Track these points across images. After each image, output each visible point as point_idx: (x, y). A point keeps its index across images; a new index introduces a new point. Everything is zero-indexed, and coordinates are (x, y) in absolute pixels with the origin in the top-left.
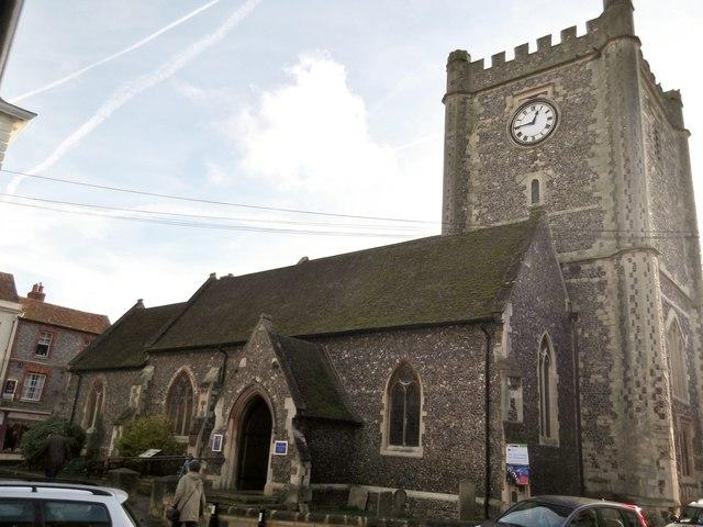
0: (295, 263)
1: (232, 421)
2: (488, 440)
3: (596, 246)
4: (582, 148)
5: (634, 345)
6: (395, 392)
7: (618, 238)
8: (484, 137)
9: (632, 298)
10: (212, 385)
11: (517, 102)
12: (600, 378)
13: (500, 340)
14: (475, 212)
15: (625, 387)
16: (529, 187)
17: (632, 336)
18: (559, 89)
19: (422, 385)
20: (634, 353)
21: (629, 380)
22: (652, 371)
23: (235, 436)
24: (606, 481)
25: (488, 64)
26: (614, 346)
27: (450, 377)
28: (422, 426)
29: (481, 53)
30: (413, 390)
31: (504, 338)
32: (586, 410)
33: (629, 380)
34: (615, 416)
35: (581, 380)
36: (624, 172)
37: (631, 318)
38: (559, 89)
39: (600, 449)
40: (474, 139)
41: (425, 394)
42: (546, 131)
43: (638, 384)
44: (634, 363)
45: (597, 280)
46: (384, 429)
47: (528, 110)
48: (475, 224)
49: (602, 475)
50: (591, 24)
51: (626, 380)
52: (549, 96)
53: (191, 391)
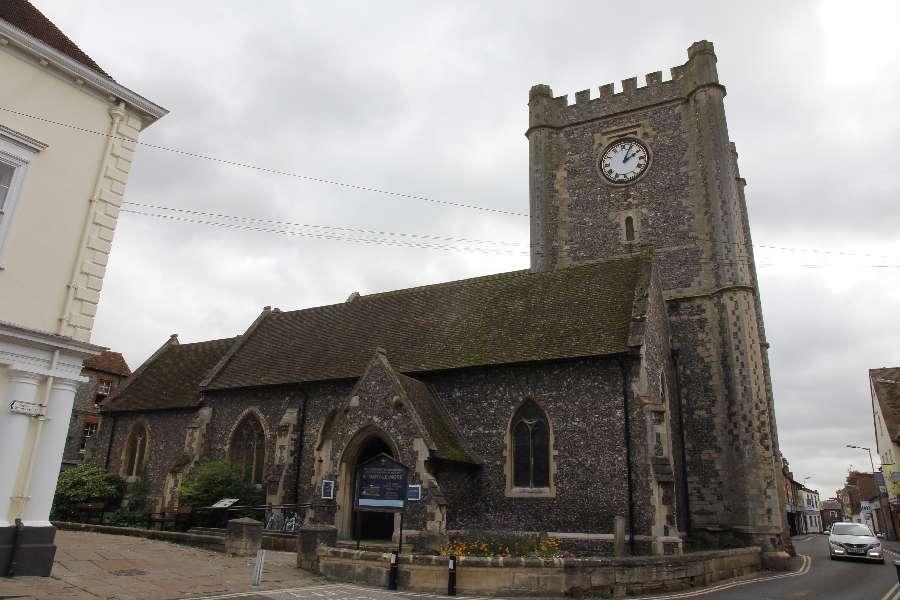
0: (343, 301)
1: (344, 465)
2: (629, 477)
4: (677, 188)
5: (738, 381)
6: (518, 430)
7: (718, 277)
8: (572, 173)
9: (735, 334)
10: (291, 429)
11: (606, 141)
12: (703, 413)
13: (637, 374)
15: (730, 422)
17: (737, 372)
18: (649, 130)
20: (739, 389)
21: (734, 414)
22: (757, 405)
23: (348, 481)
24: (712, 513)
25: (572, 101)
26: (716, 381)
27: (583, 413)
29: (565, 88)
30: (541, 430)
31: (643, 373)
32: (690, 445)
33: (734, 414)
34: (719, 450)
35: (685, 415)
36: (721, 213)
37: (735, 354)
38: (649, 130)
39: (705, 483)
40: (561, 174)
41: (555, 432)
42: (638, 170)
43: (744, 418)
44: (739, 398)
45: (697, 317)
46: (508, 470)
47: (619, 148)
48: (565, 262)
49: (709, 508)
50: (675, 71)
51: (731, 415)
53: (261, 435)
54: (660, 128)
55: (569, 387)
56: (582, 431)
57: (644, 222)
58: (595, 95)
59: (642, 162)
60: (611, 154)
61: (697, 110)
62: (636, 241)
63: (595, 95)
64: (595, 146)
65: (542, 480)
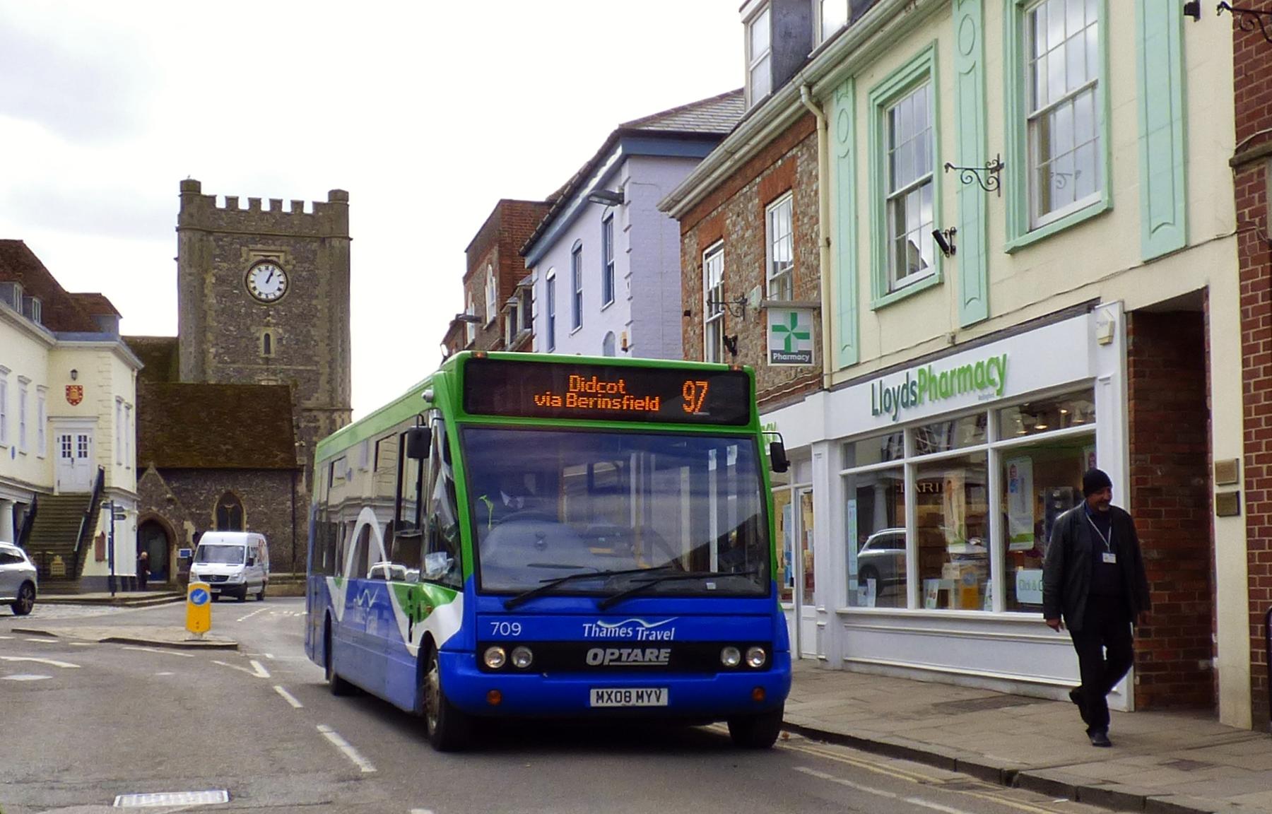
3: (313, 399)
4: (307, 317)
7: (332, 398)
8: (221, 280)
14: (213, 350)
16: (263, 339)
25: (221, 204)
27: (267, 504)
29: (217, 187)
42: (278, 293)
47: (263, 267)
50: (317, 205)
52: (281, 262)
54: (301, 259)
55: (257, 485)
56: (265, 514)
58: (244, 205)
59: (282, 286)
60: (256, 271)
61: (331, 255)
62: (273, 355)
63: (244, 205)
64: (242, 260)
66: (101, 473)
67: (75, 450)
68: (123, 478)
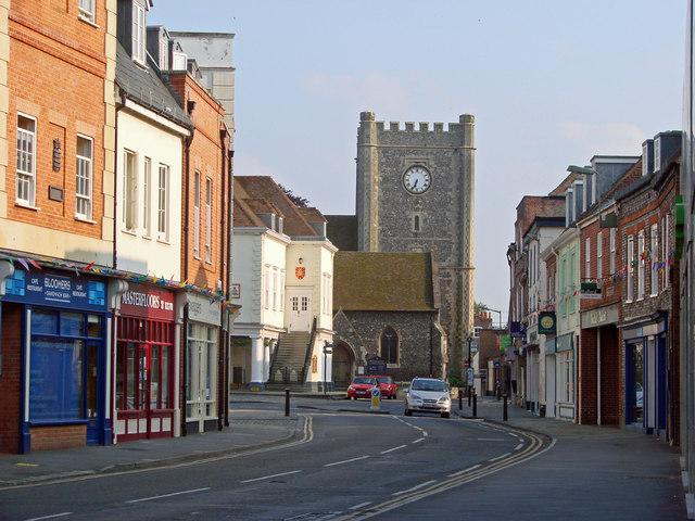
4: (443, 204)
6: (384, 341)
11: (408, 165)
19: (400, 337)
20: (464, 317)
28: (400, 356)
29: (384, 116)
30: (395, 340)
50: (451, 126)
57: (425, 220)
58: (402, 127)
65: (394, 360)
66: (315, 321)
67: (300, 306)
68: (326, 322)
